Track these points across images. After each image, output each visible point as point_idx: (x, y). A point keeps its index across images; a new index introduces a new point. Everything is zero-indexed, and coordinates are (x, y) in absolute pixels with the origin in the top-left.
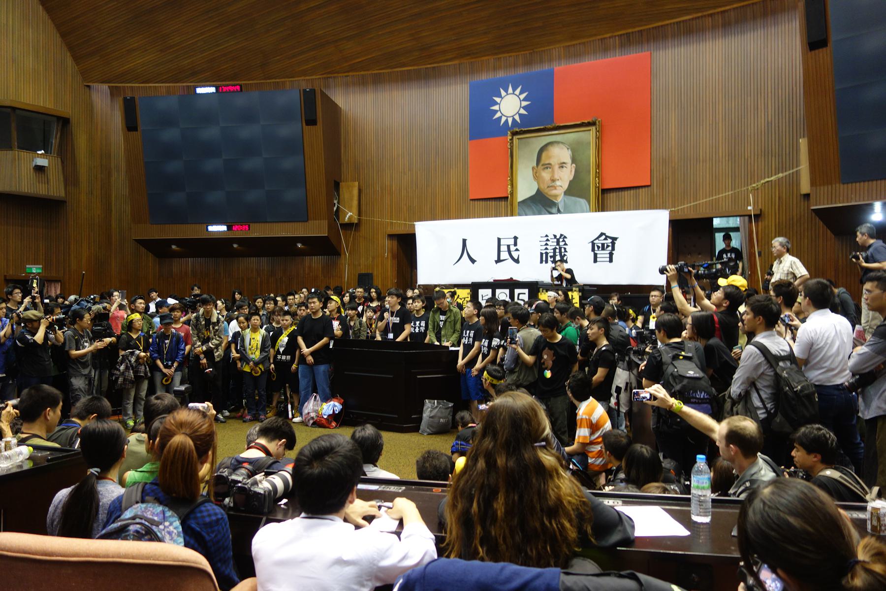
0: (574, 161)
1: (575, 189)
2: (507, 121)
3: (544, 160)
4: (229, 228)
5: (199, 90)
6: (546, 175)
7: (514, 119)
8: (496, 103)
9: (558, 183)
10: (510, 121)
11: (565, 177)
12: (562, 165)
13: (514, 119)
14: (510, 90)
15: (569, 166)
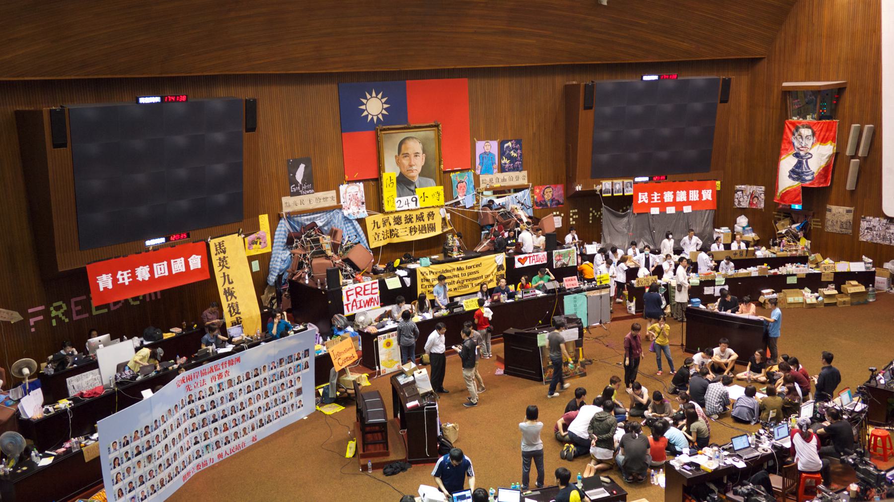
0: (424, 152)
1: (425, 172)
2: (372, 119)
3: (403, 151)
4: (167, 239)
5: (142, 100)
6: (405, 162)
7: (378, 118)
8: (363, 104)
9: (414, 168)
10: (375, 119)
11: (419, 163)
12: (416, 155)
13: (378, 118)
14: (374, 94)
15: (421, 155)
